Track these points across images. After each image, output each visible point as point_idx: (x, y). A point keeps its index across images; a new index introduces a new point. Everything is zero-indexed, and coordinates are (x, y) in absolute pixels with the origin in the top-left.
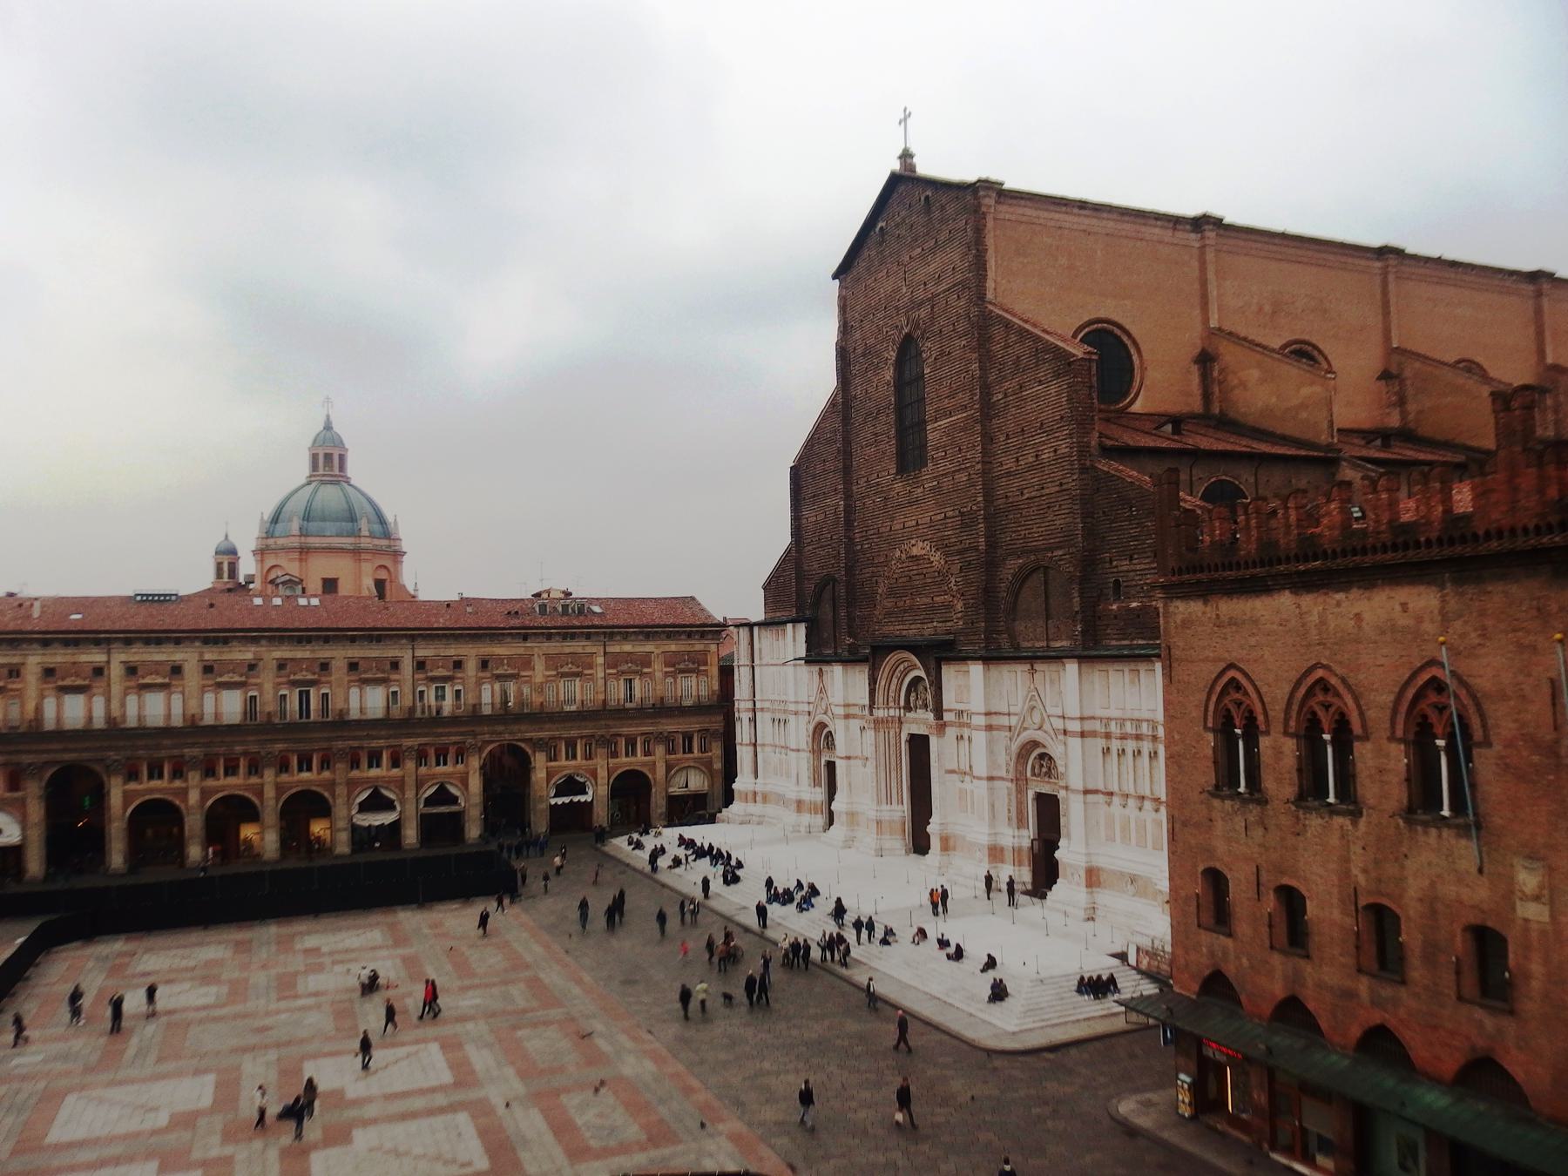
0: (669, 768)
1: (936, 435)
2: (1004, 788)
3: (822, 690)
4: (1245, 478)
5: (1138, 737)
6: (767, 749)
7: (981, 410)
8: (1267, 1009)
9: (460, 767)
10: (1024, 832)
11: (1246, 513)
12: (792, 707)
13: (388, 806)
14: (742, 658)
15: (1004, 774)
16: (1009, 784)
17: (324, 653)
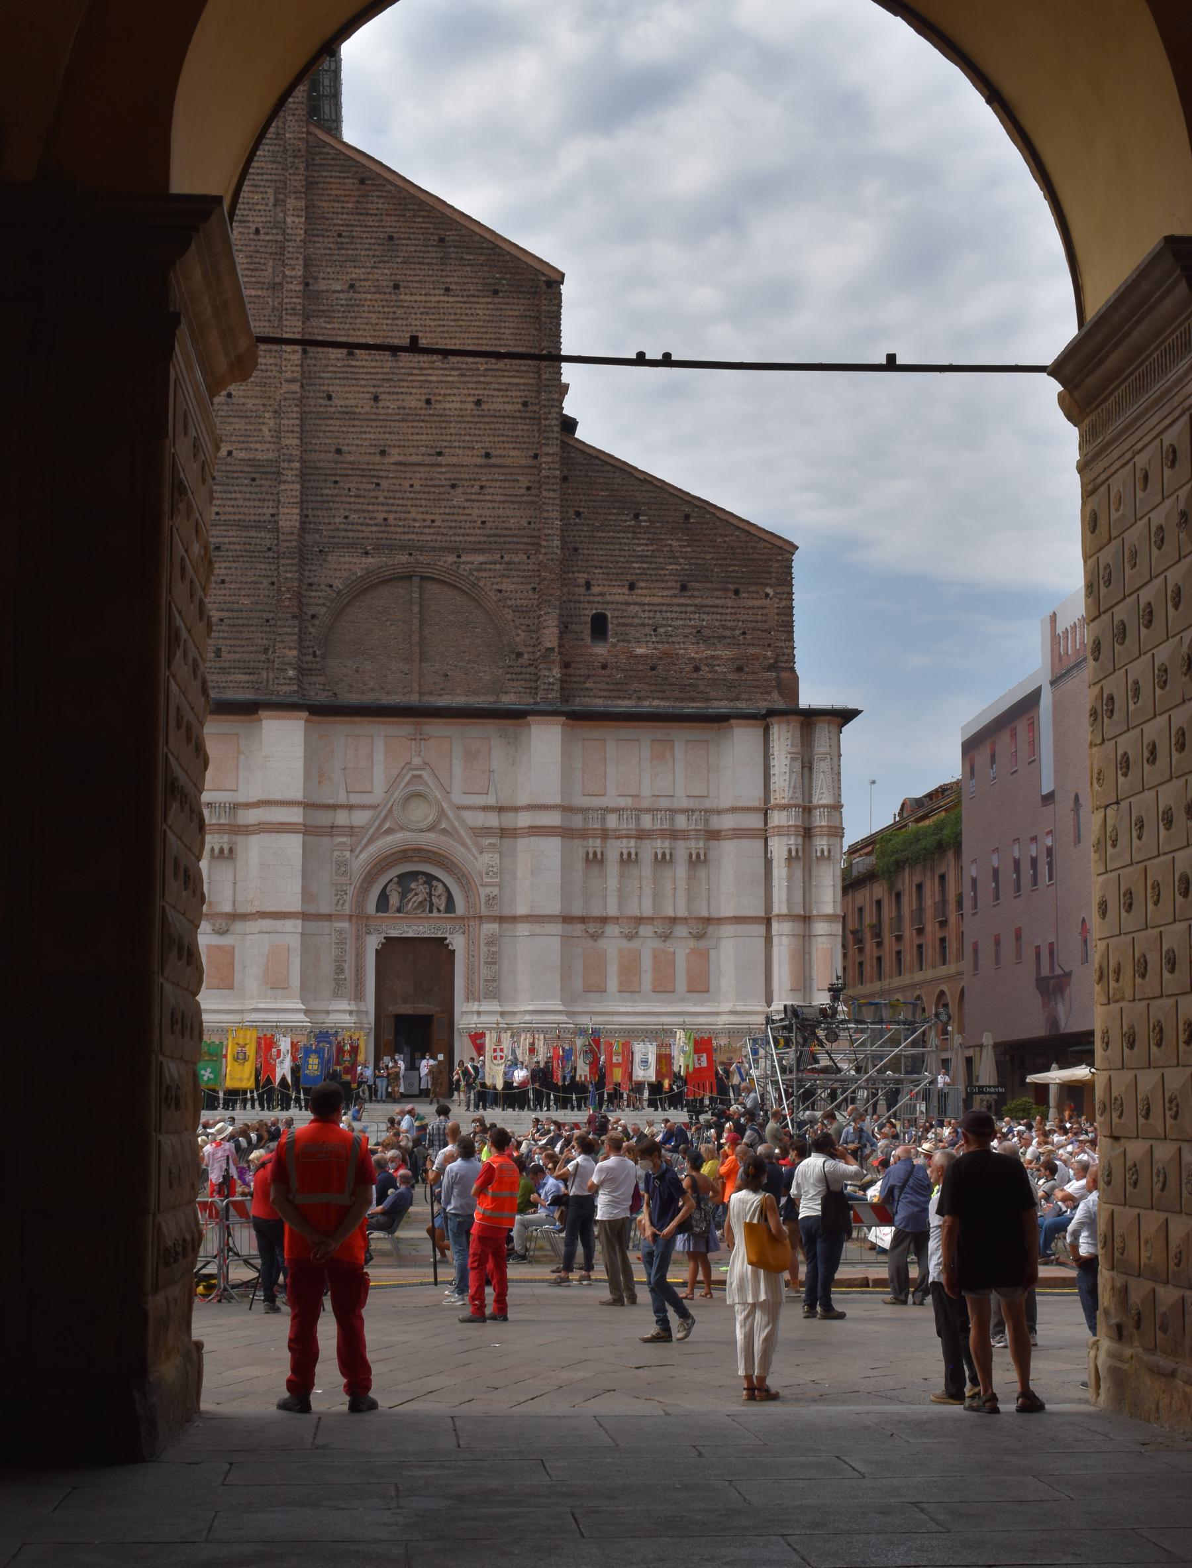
16: (346, 925)
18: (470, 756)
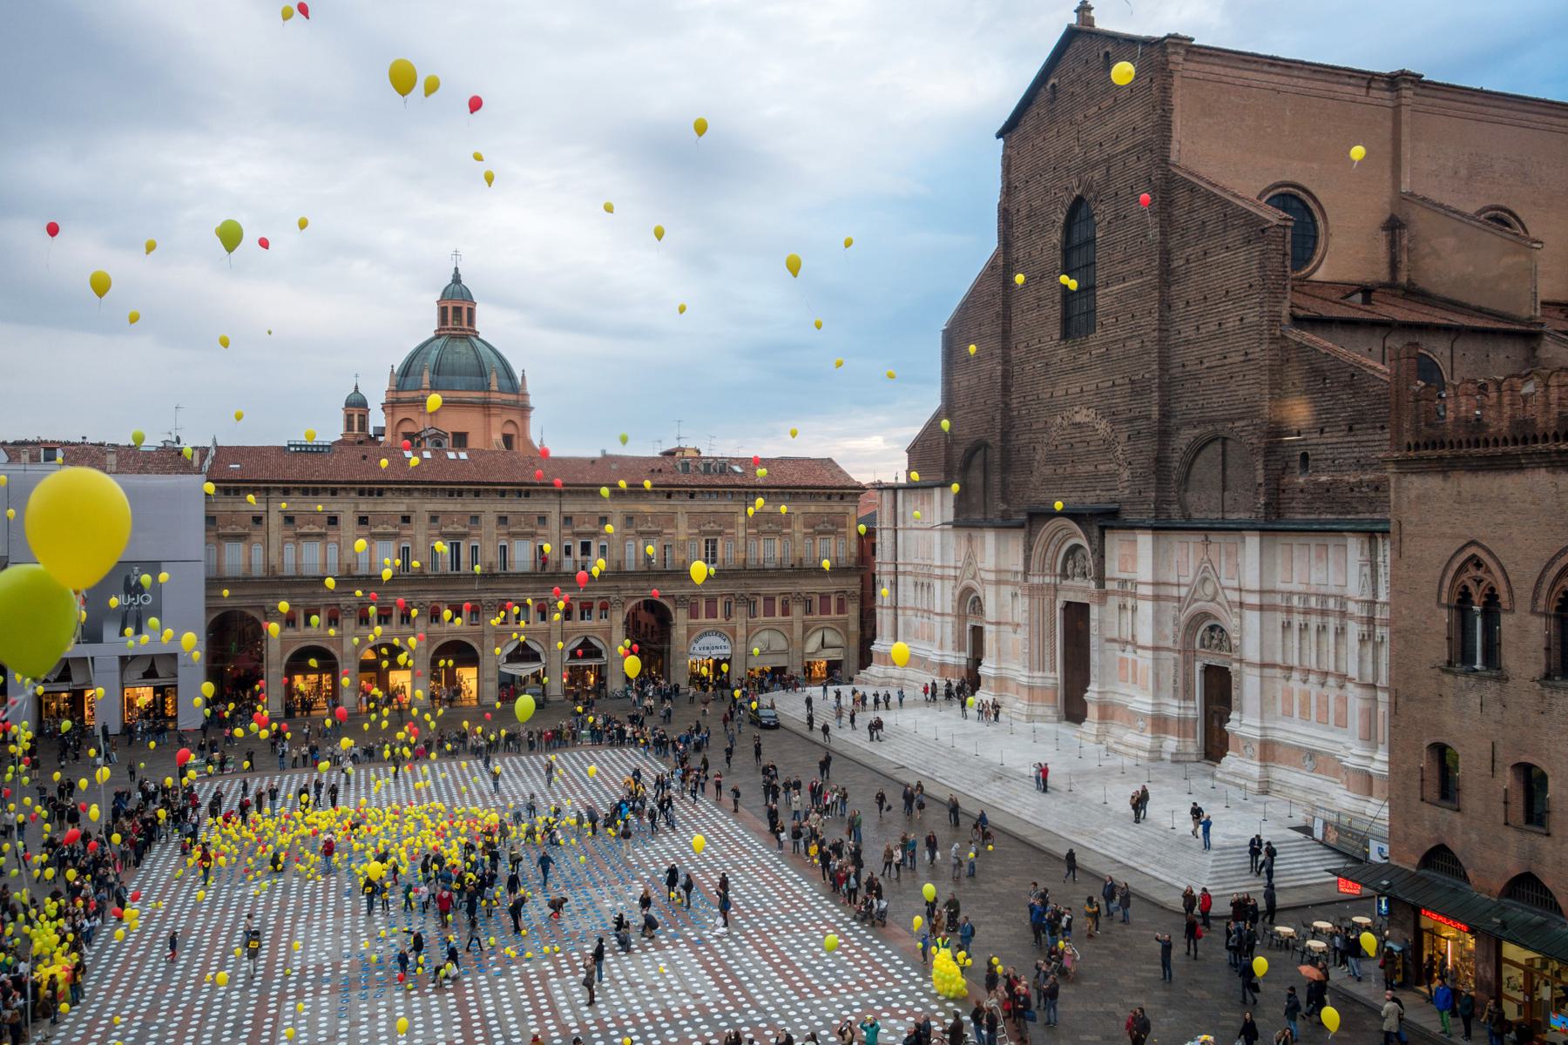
0: (806, 629)
1: (1108, 300)
2: (1169, 658)
3: (970, 558)
4: (1438, 350)
5: (1324, 613)
6: (909, 612)
7: (1161, 275)
8: (1498, 885)
9: (604, 621)
10: (1191, 704)
11: (1499, 389)
12: (938, 572)
13: (535, 657)
14: (885, 520)
15: (1170, 643)
17: (474, 505)
18: (1228, 555)
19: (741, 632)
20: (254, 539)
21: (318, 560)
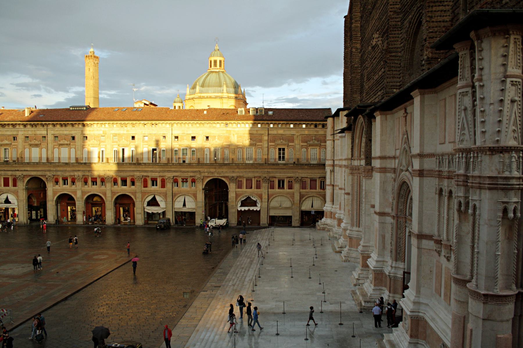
0: (301, 196)
19: (265, 197)
20: (43, 146)
21: (67, 156)
